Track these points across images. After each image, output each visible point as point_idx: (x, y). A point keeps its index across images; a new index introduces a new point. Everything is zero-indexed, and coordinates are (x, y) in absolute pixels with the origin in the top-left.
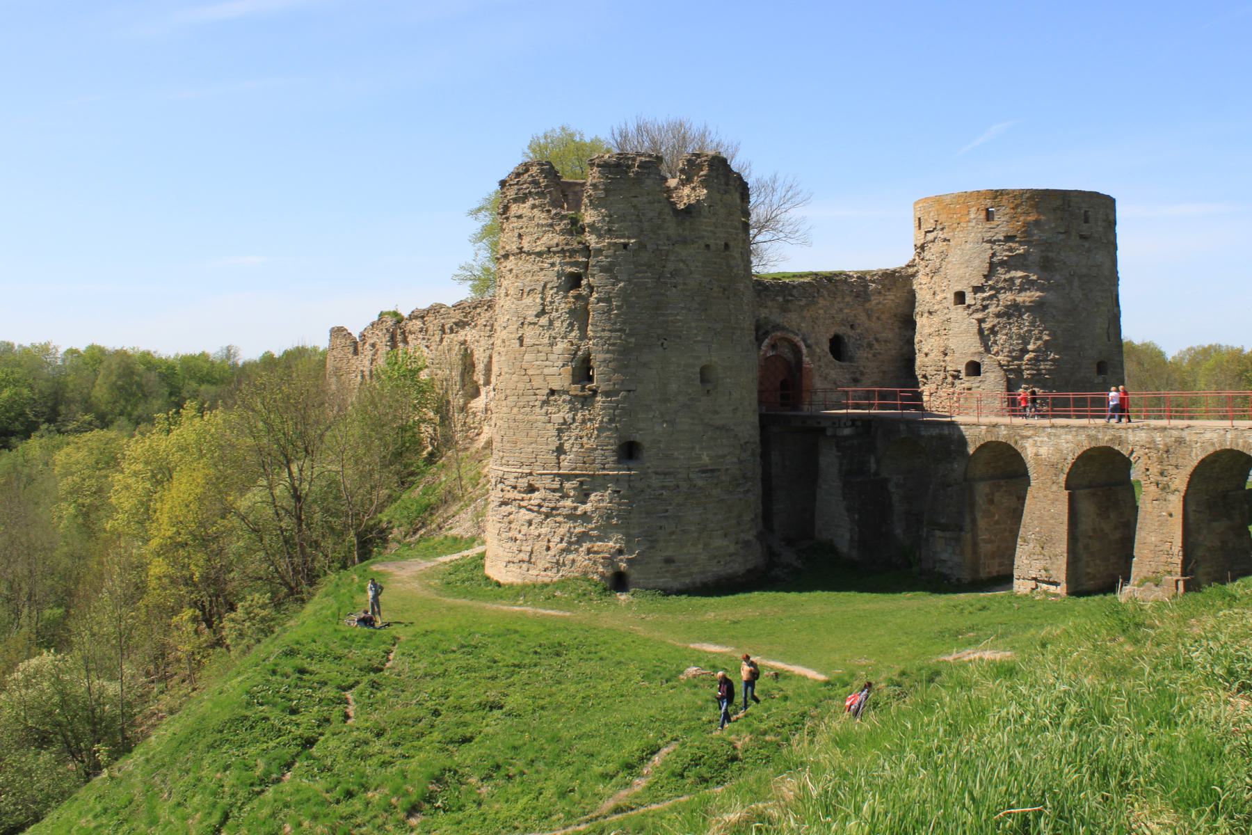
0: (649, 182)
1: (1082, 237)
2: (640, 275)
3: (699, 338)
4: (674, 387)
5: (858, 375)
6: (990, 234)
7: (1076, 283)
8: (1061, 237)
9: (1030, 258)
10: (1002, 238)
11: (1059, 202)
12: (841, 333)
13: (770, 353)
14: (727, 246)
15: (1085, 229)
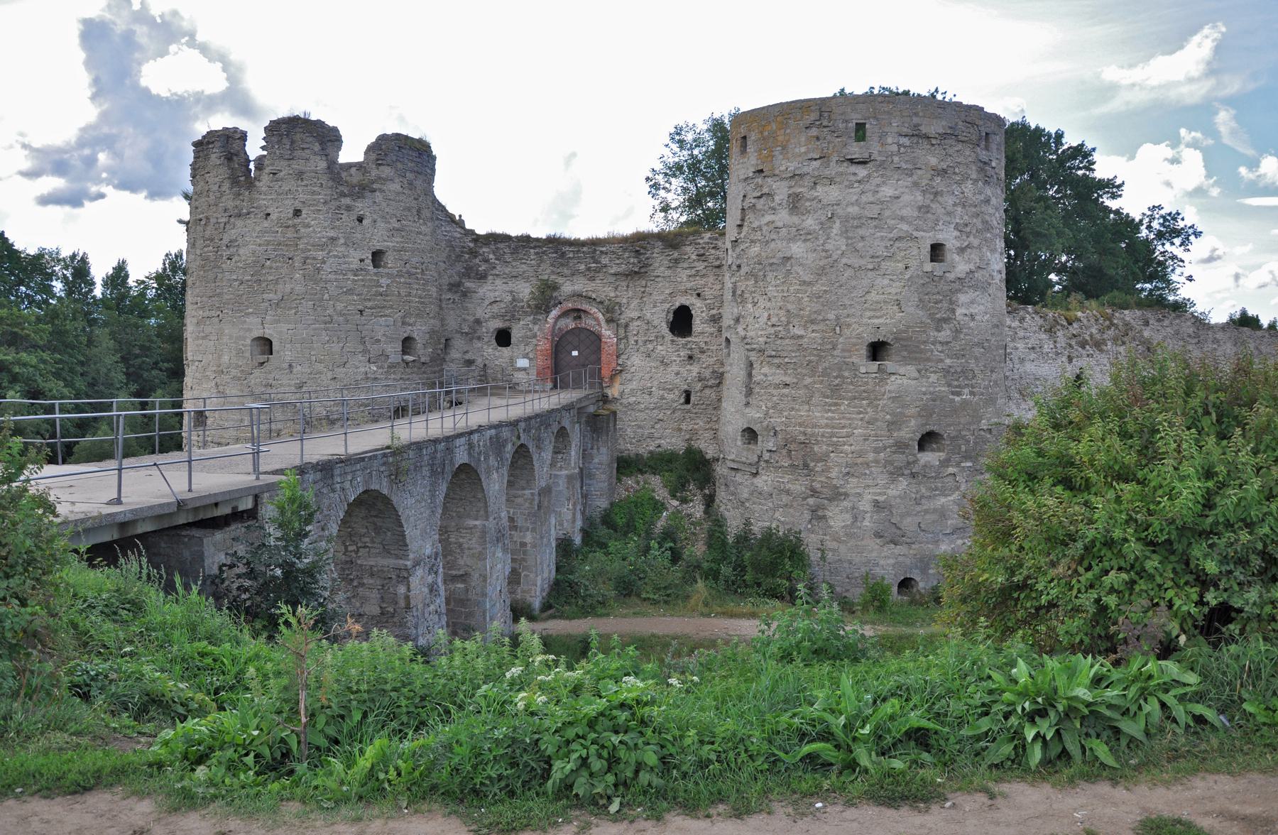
0: (213, 156)
1: (851, 161)
2: (206, 249)
3: (251, 310)
4: (226, 358)
5: (696, 352)
6: (743, 171)
7: (837, 227)
8: (816, 164)
9: (777, 198)
10: (751, 175)
11: (814, 116)
12: (687, 303)
13: (572, 325)
14: (297, 213)
15: (856, 150)
